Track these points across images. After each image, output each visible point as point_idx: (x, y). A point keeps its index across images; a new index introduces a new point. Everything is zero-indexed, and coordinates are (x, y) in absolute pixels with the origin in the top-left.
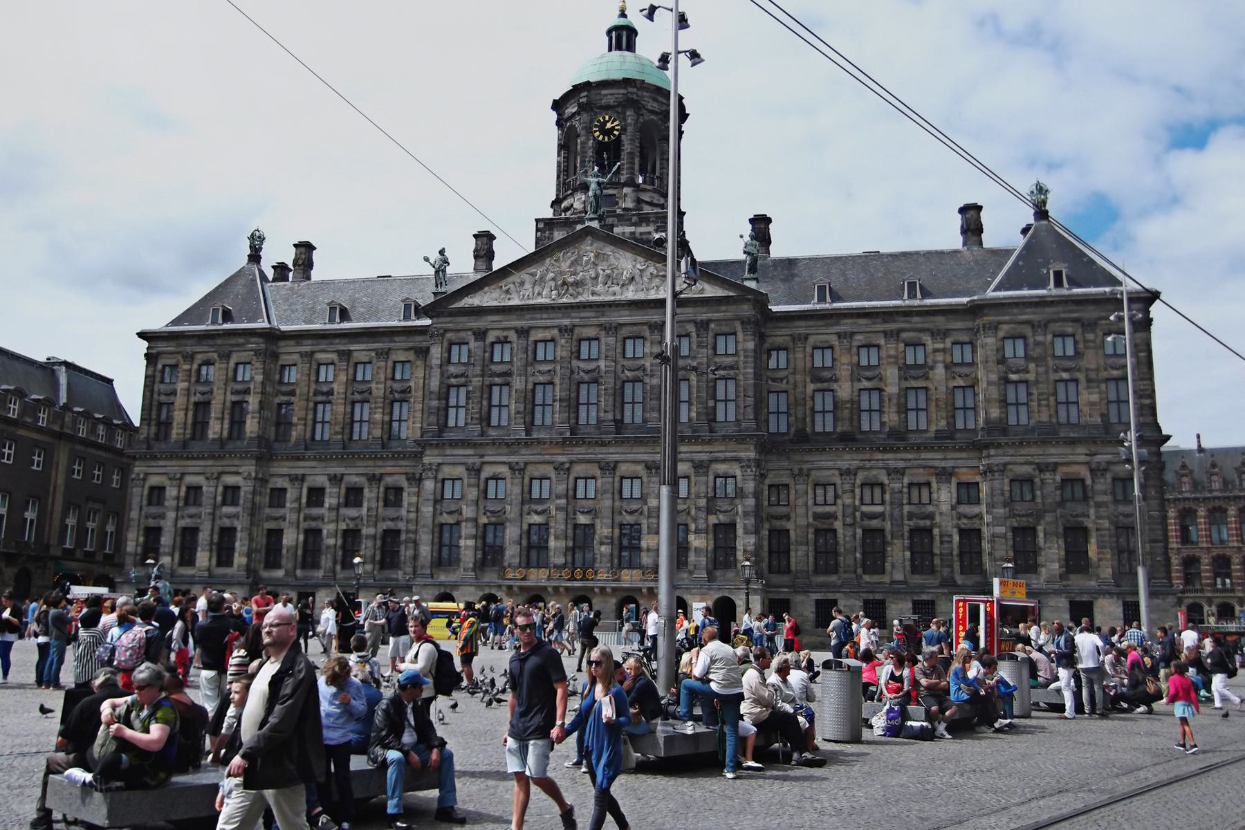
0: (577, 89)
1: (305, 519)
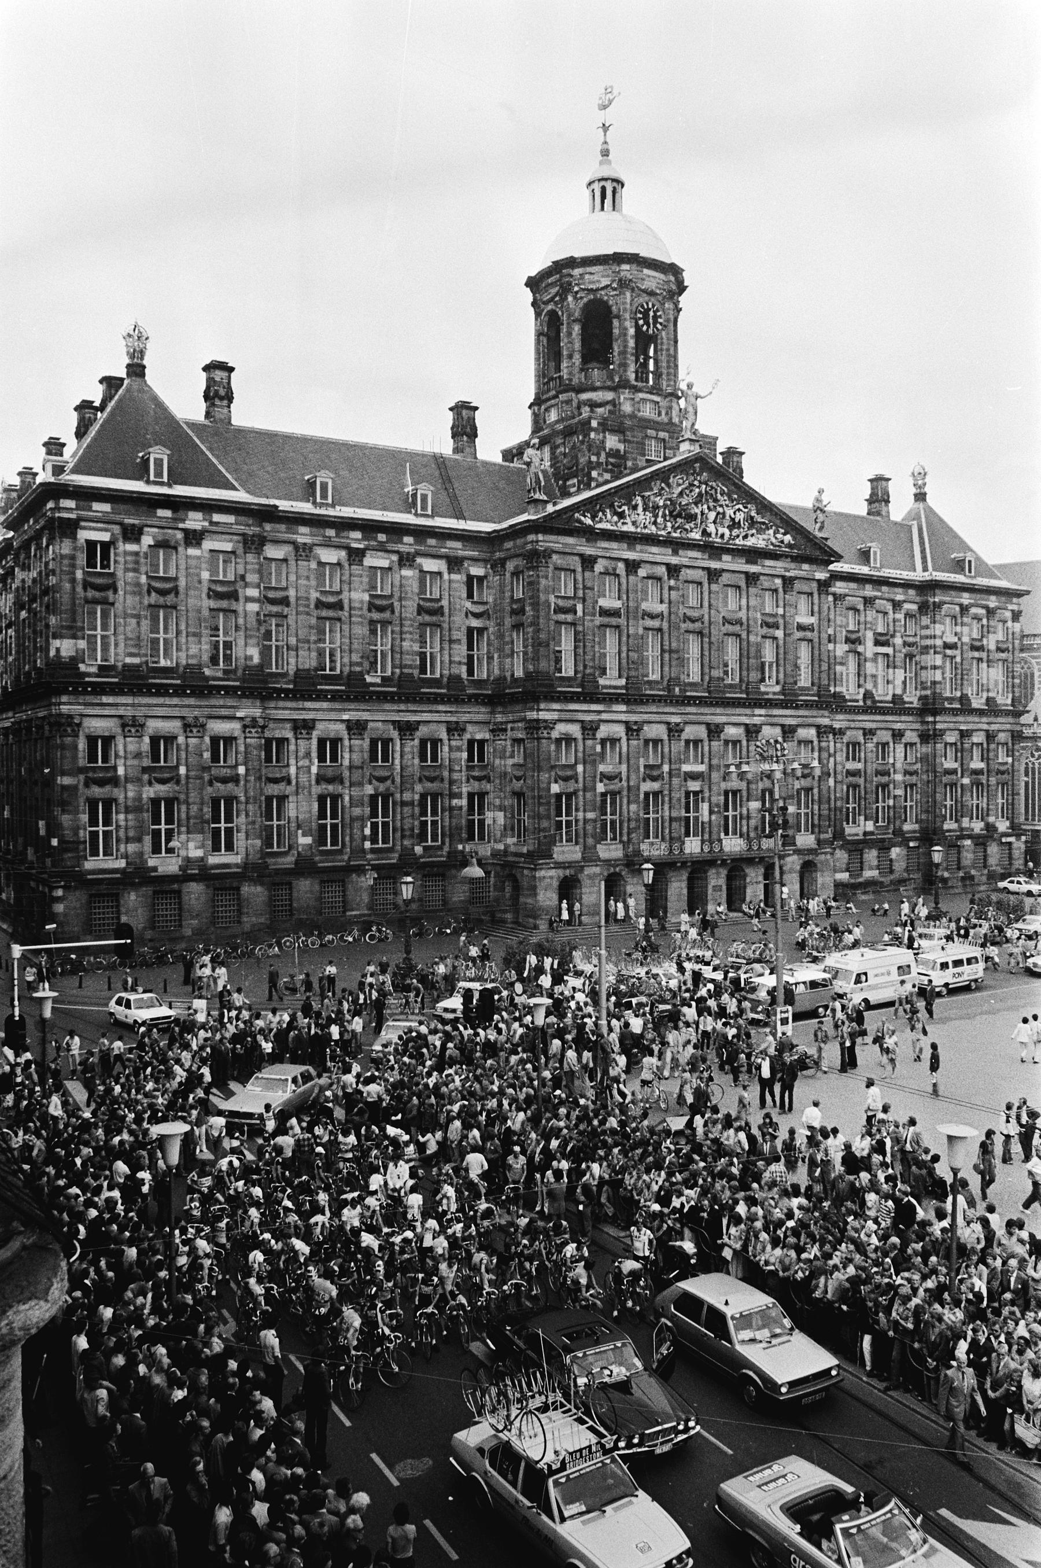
0: (618, 258)
1: (318, 782)
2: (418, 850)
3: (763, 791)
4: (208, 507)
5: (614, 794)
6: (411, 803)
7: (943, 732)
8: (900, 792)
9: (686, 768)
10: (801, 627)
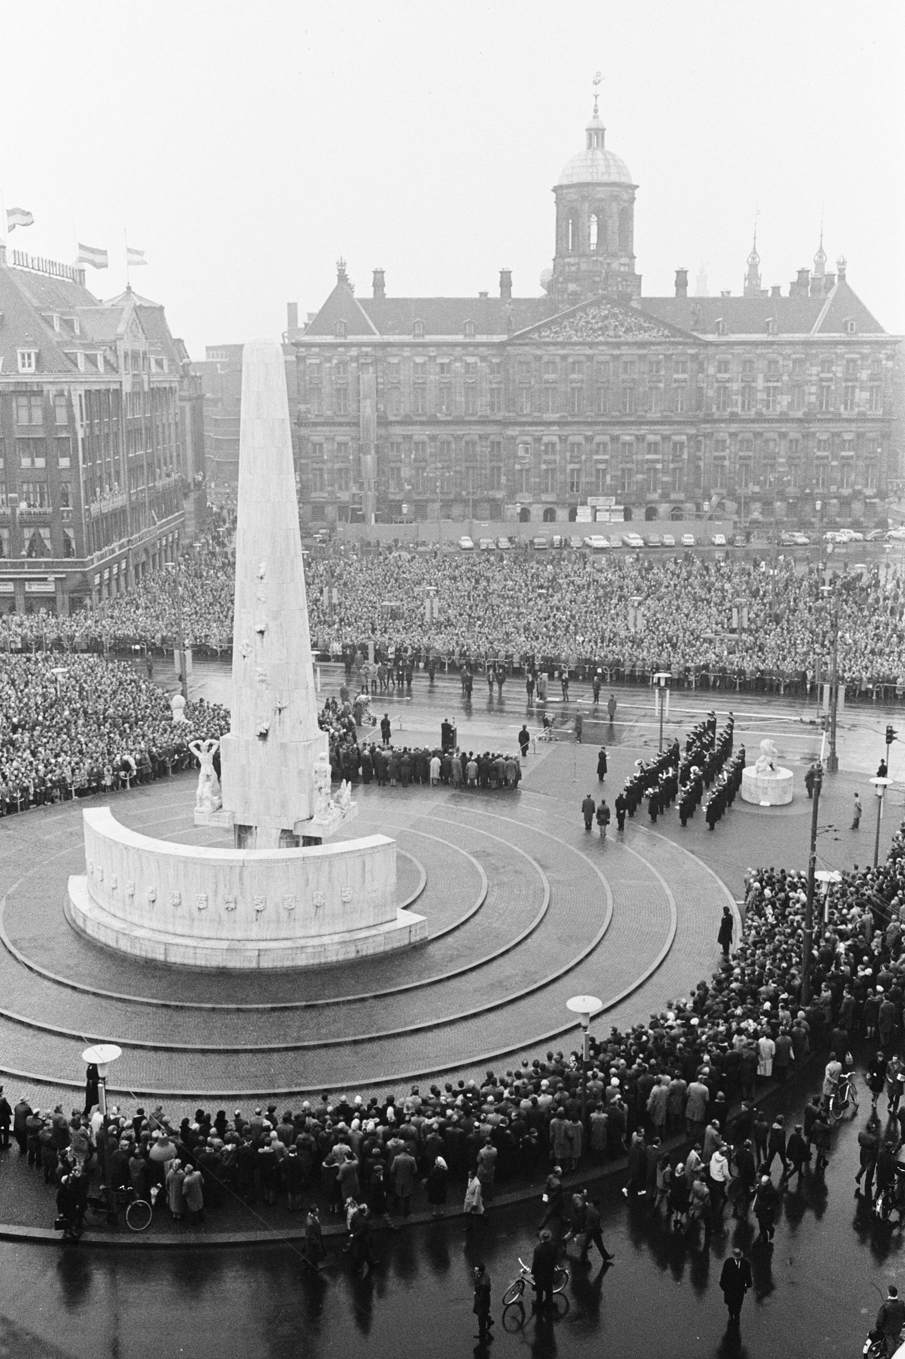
2: (464, 493)
3: (649, 469)
4: (359, 345)
5: (553, 470)
6: (460, 472)
7: (814, 434)
8: (781, 469)
9: (595, 457)
10: (676, 381)
